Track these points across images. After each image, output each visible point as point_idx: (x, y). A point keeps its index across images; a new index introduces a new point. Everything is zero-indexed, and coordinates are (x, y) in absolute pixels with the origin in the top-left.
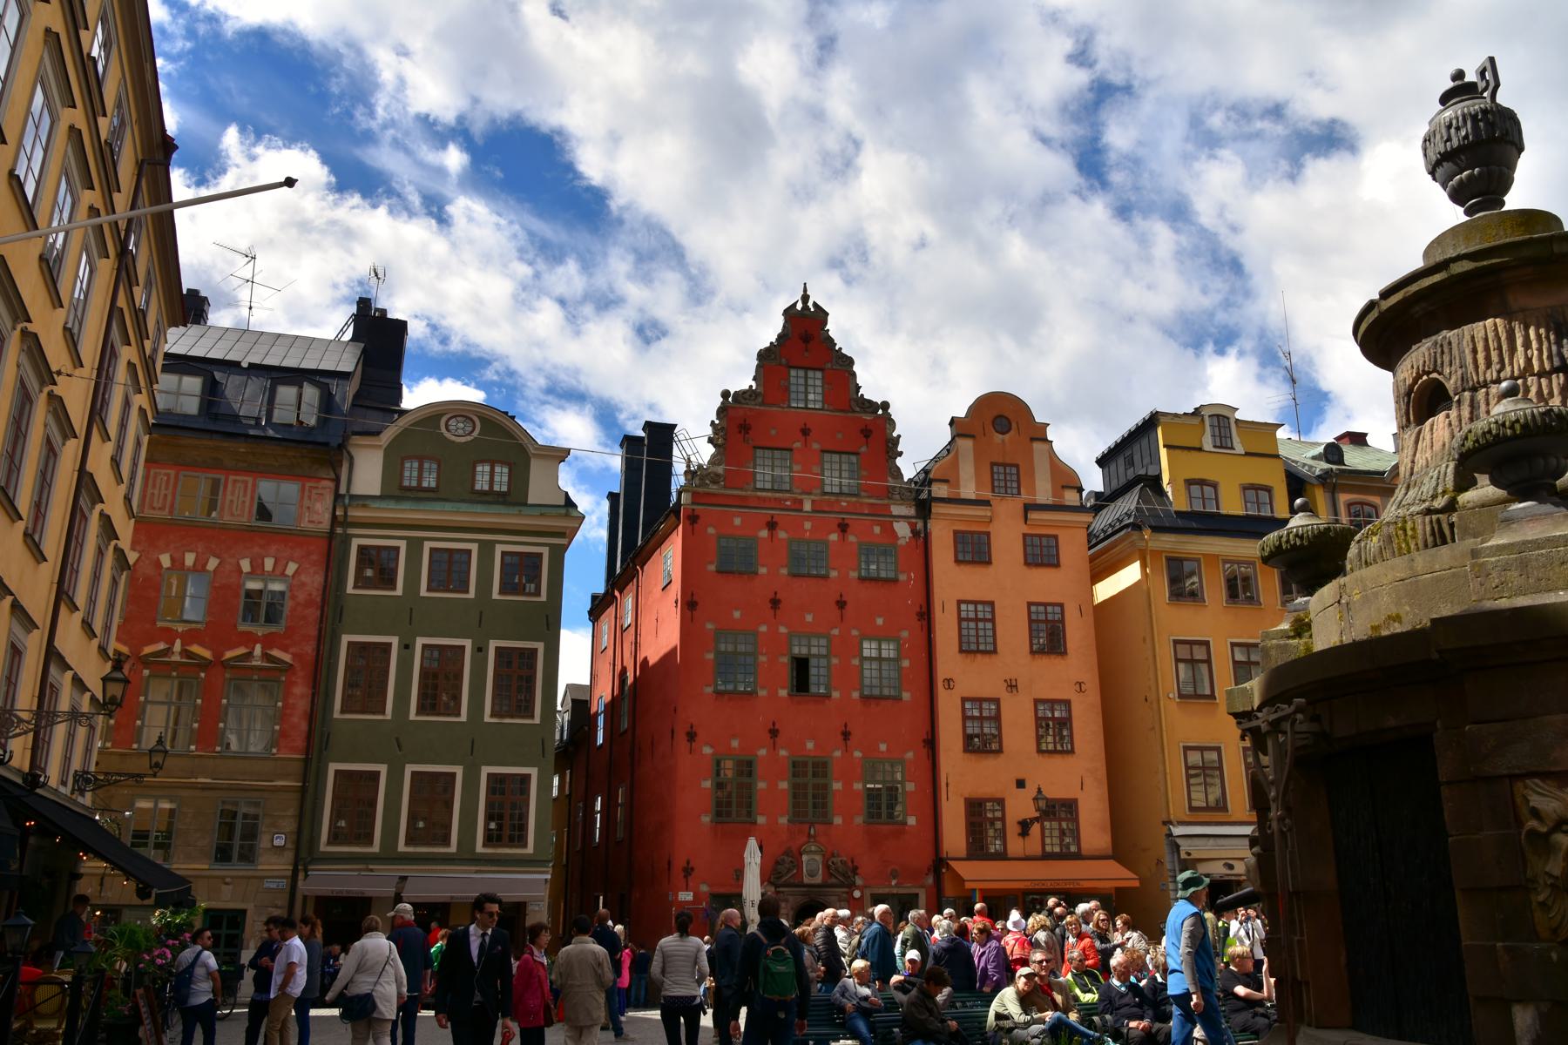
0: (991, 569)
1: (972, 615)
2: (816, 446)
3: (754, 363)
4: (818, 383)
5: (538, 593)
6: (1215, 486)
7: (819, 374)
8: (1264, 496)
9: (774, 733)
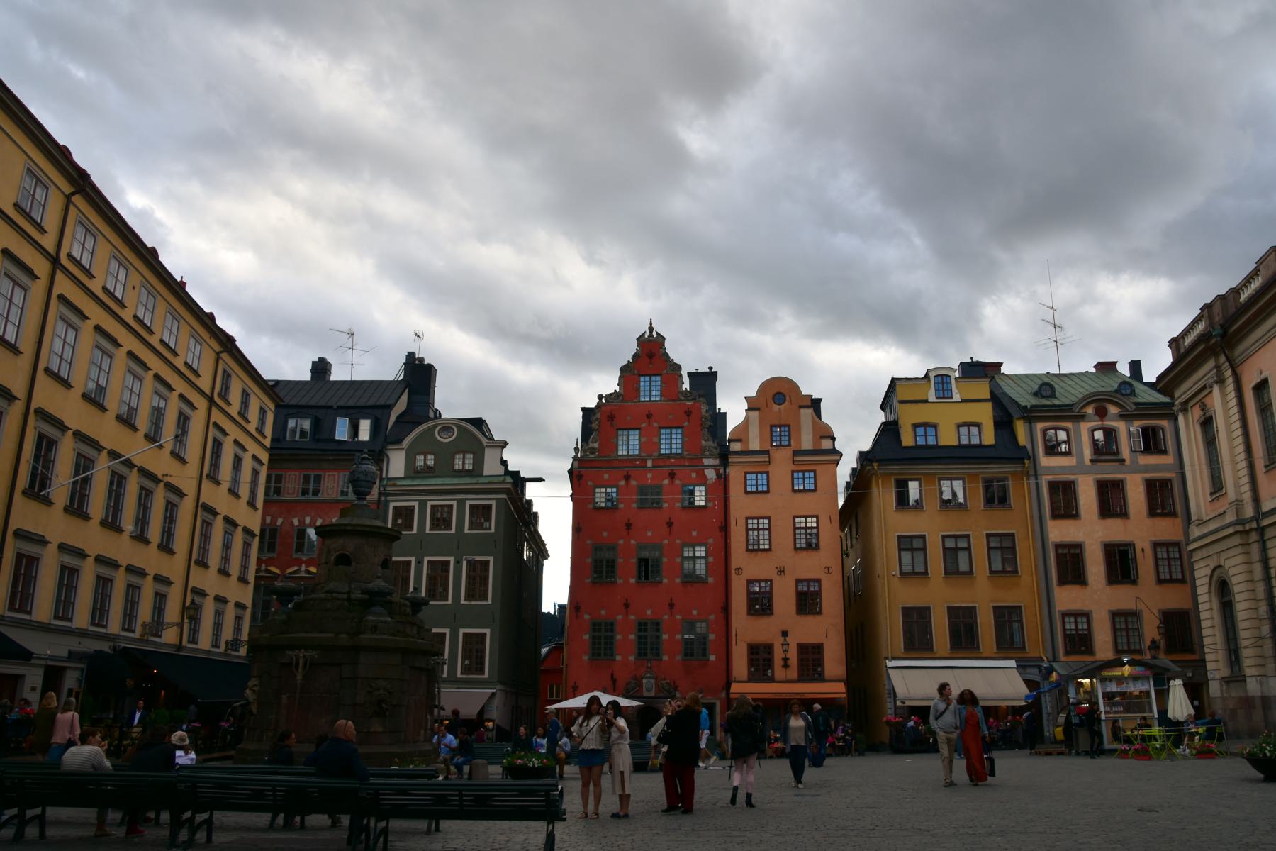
0: (768, 496)
2: (655, 425)
6: (935, 426)
7: (659, 378)
8: (974, 430)
9: (627, 605)
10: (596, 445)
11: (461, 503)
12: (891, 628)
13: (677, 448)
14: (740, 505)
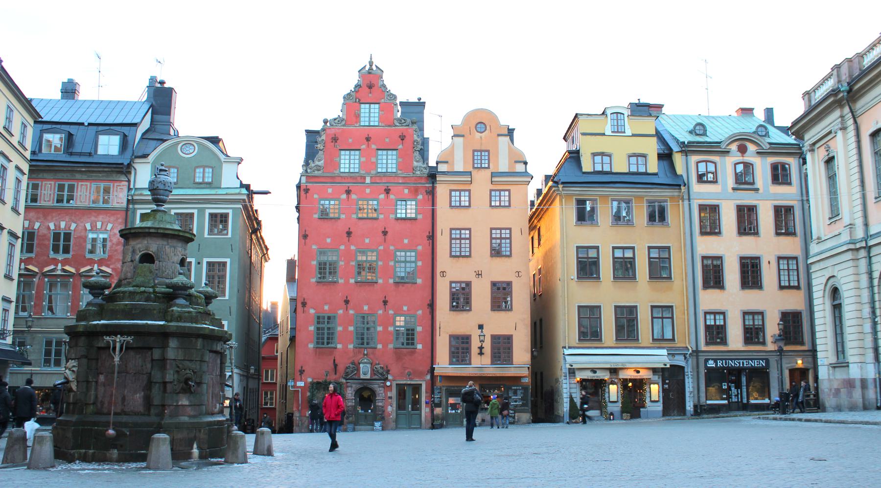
0: (470, 210)
1: (458, 236)
2: (374, 147)
3: (342, 101)
4: (377, 111)
5: (227, 234)
7: (377, 106)
9: (347, 302)
10: (321, 163)
11: (201, 211)
12: (566, 326)
13: (392, 168)
14: (446, 218)
